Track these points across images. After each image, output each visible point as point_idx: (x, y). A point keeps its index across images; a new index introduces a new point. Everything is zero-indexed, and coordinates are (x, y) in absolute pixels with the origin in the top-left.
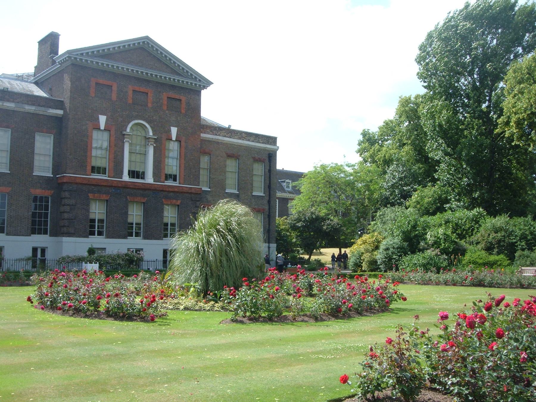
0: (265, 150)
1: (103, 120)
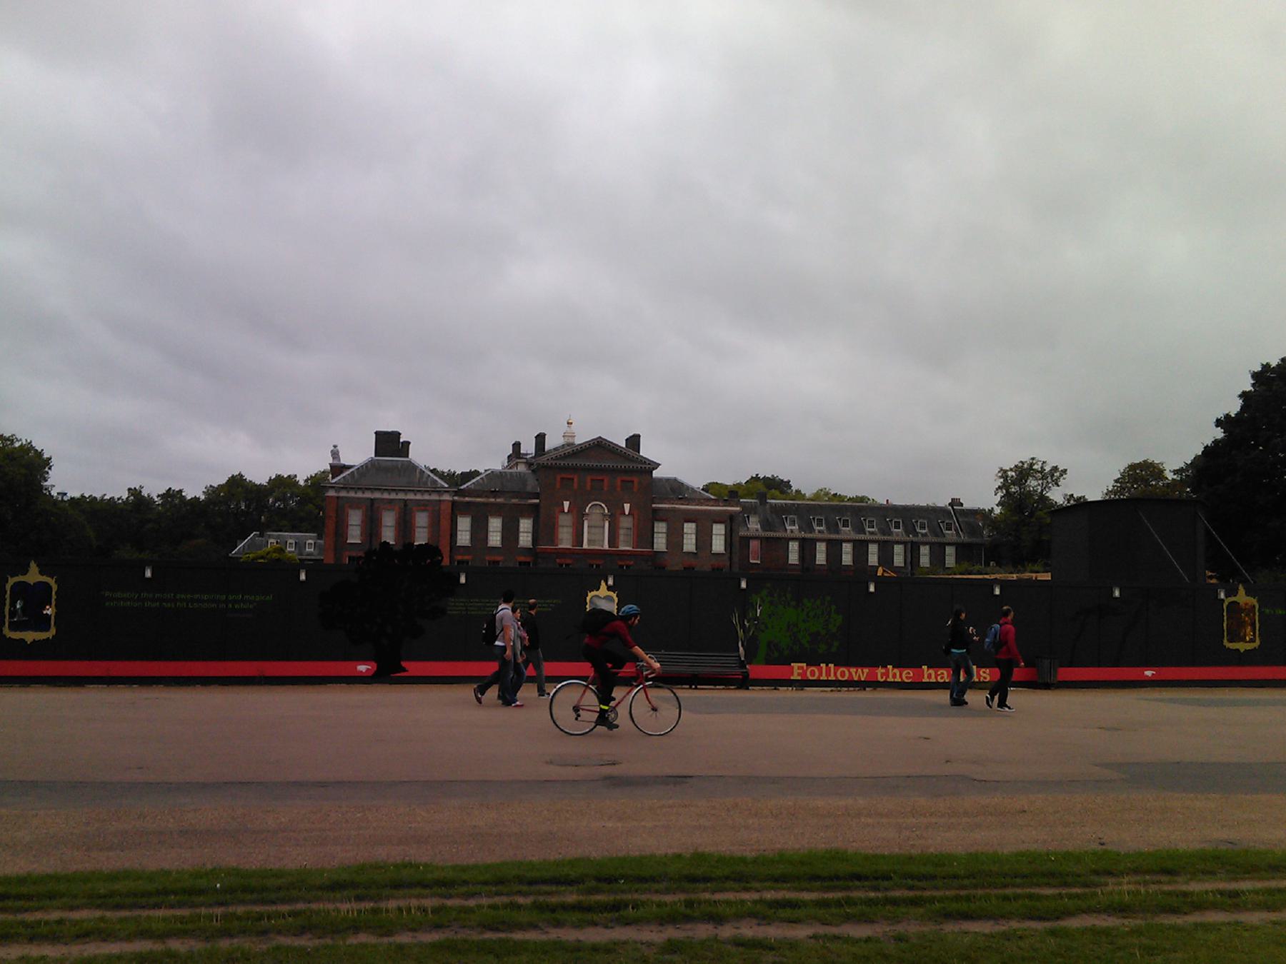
1: (566, 504)
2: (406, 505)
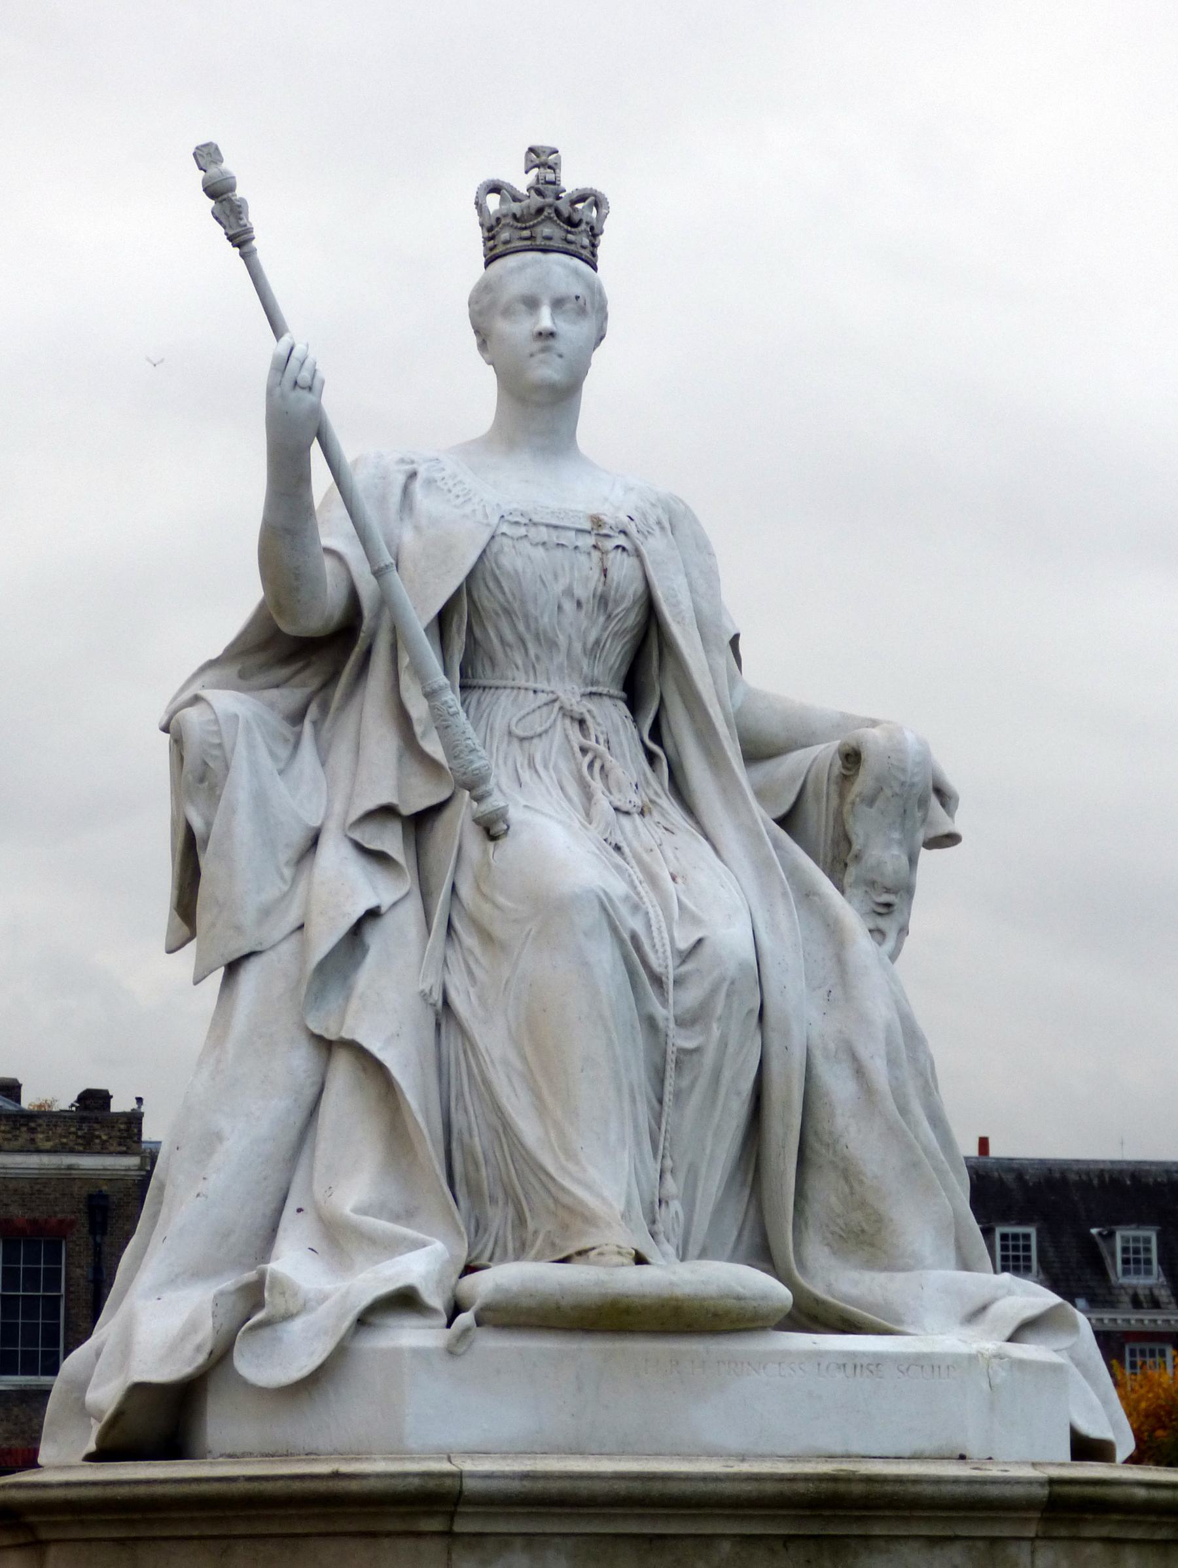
0: (66, 1179)
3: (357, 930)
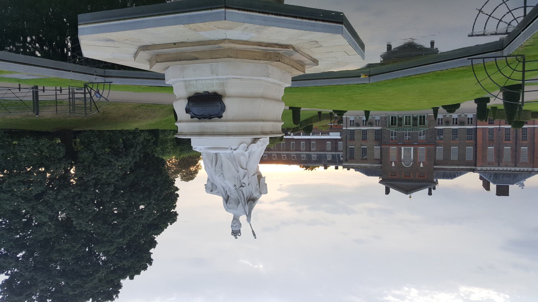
0: (349, 163)
1: (422, 165)
2: (499, 164)
3: (244, 177)
